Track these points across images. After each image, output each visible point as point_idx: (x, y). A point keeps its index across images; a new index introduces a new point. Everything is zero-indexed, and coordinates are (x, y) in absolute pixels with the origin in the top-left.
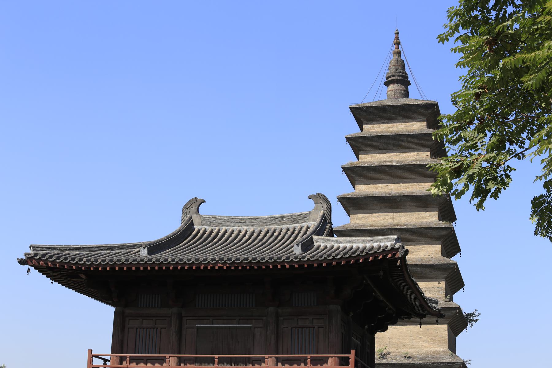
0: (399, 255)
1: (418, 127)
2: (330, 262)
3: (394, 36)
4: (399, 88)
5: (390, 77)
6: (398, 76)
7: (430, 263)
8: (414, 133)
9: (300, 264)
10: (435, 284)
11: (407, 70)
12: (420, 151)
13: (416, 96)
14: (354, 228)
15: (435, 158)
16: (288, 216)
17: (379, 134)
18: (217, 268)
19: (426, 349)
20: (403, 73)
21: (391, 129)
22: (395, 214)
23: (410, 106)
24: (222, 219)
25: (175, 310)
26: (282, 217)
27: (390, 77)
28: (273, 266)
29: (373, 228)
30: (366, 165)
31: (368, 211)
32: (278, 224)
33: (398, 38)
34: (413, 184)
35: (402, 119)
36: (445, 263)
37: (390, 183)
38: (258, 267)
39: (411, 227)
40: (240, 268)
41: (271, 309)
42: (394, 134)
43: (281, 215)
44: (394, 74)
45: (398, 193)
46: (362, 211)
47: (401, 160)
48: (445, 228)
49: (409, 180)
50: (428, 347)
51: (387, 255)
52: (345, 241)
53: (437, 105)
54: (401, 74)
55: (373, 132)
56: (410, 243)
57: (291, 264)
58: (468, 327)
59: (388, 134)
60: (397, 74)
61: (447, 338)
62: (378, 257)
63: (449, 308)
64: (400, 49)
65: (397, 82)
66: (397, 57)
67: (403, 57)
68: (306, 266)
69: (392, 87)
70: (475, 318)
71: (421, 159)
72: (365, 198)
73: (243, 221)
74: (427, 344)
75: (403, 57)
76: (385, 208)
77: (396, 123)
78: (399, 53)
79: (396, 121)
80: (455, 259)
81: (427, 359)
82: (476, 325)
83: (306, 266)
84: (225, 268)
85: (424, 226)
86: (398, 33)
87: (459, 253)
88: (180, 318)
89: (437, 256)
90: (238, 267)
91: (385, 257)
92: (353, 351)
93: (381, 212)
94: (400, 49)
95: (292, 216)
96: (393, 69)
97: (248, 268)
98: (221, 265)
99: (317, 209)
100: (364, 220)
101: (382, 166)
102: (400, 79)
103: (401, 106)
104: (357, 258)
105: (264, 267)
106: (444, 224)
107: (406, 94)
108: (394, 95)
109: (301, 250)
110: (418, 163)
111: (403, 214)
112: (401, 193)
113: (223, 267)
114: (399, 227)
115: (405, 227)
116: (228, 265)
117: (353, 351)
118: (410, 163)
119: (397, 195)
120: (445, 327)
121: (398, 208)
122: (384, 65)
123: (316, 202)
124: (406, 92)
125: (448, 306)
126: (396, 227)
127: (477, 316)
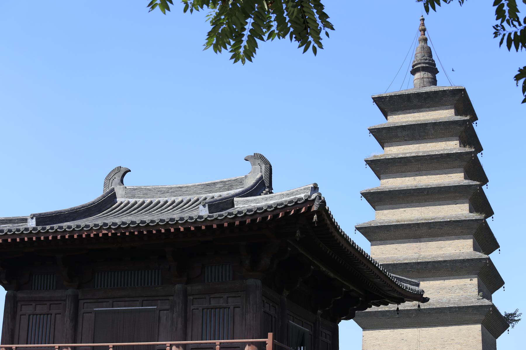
0: (315, 208)
1: (446, 114)
2: (232, 221)
3: (420, 22)
4: (426, 76)
6: (424, 63)
7: (460, 258)
8: (441, 121)
9: (196, 225)
10: (467, 281)
11: (434, 58)
12: (449, 140)
13: (445, 82)
14: (379, 224)
15: (464, 147)
16: (221, 182)
17: (404, 124)
18: (101, 235)
20: (430, 60)
21: (417, 119)
22: (423, 208)
23: (436, 93)
24: (148, 189)
25: (70, 292)
28: (165, 230)
29: (398, 223)
30: (390, 157)
31: (394, 206)
32: (210, 192)
33: (423, 25)
34: (441, 176)
35: (429, 107)
36: (477, 257)
37: (417, 175)
38: (147, 231)
39: (439, 220)
40: (127, 234)
41: (178, 287)
42: (419, 123)
43: (213, 182)
44: (419, 61)
45: (425, 185)
46: (388, 206)
47: (429, 150)
48: (476, 220)
49: (437, 171)
51: (301, 209)
52: (263, 199)
53: (464, 90)
54: (427, 61)
55: (397, 123)
56: (439, 238)
57: (186, 226)
58: (510, 328)
59: (413, 123)
60: (423, 61)
61: (480, 338)
62: (290, 212)
63: (482, 306)
64: (426, 36)
65: (424, 69)
66: (423, 44)
67: (429, 44)
68: (203, 227)
69: (418, 75)
70: (516, 318)
71: (449, 148)
72: (390, 192)
73: (170, 191)
76: (412, 202)
77: (422, 112)
78: (425, 40)
79: (422, 110)
80: (494, 257)
82: (517, 325)
83: (203, 227)
84: (110, 234)
85: (453, 219)
87: (498, 250)
88: (76, 301)
89: (468, 251)
90: (125, 233)
91: (298, 211)
92: (270, 335)
93: (408, 207)
94: (426, 36)
96: (419, 56)
97: (136, 233)
98: (106, 232)
99: (254, 172)
100: (391, 216)
102: (428, 67)
103: (426, 93)
104: (264, 215)
105: (154, 232)
106: (475, 216)
107: (434, 82)
109: (208, 212)
110: (445, 152)
111: (431, 208)
112: (429, 185)
113: (108, 234)
114: (426, 221)
115: (432, 221)
116: (113, 231)
117: (270, 335)
118: (437, 153)
119: (424, 187)
120: (479, 327)
121: (426, 201)
122: (412, 54)
123: (253, 164)
124: (433, 80)
125: (481, 304)
126: (423, 221)
127: (518, 316)
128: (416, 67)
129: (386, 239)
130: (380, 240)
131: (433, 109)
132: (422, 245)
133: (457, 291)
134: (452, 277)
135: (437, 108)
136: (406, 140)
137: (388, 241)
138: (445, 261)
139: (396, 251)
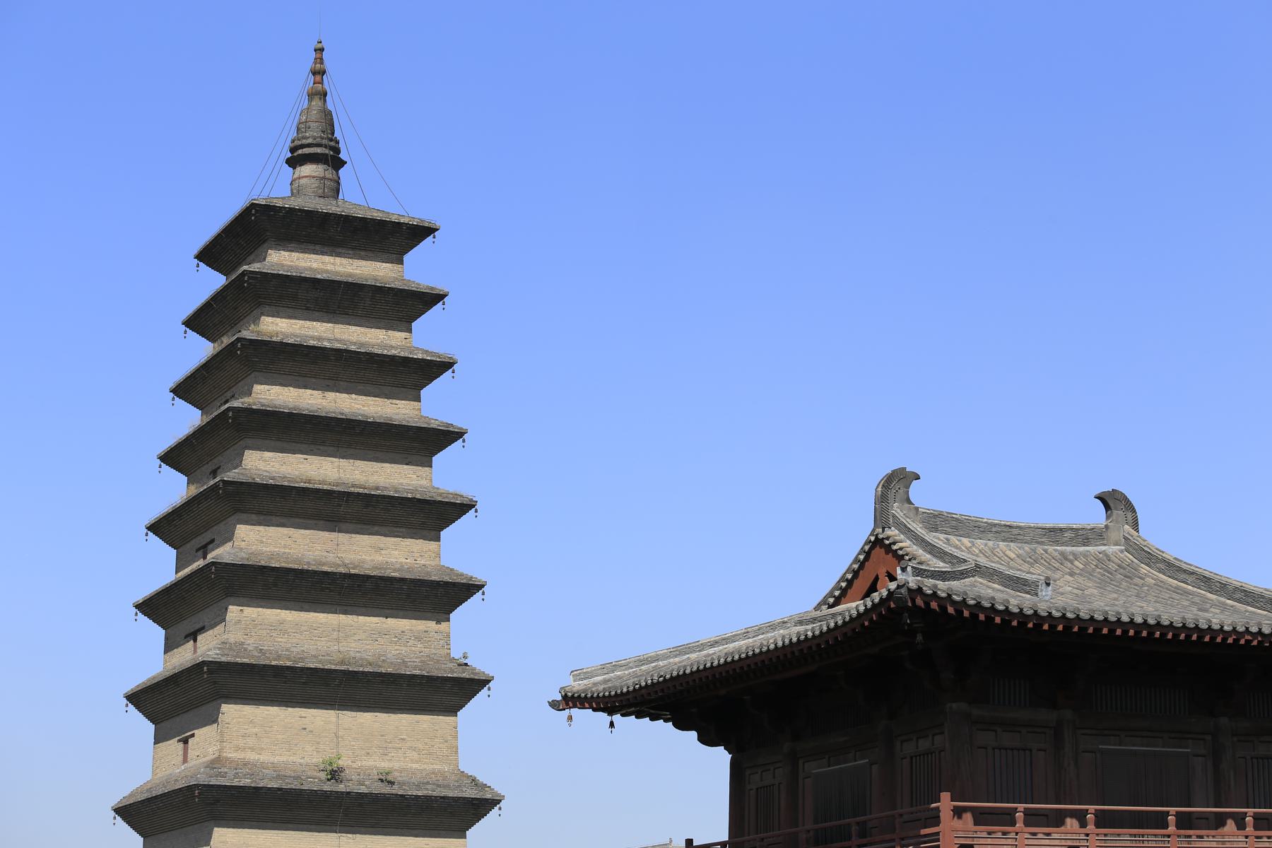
5: (302, 146)
6: (326, 147)
17: (319, 277)
19: (415, 766)
20: (331, 140)
26: (1061, 529)
27: (302, 146)
29: (311, 486)
35: (353, 248)
42: (350, 280)
50: (417, 762)
59: (338, 278)
72: (290, 415)
74: (415, 755)
75: (330, 106)
81: (429, 787)
85: (418, 496)
86: (322, 50)
95: (1077, 530)
100: (277, 466)
101: (325, 349)
108: (318, 187)
114: (366, 491)
115: (379, 492)
128: (300, 152)
129: (270, 513)
130: (259, 513)
131: (363, 253)
132: (342, 537)
133: (411, 642)
134: (401, 613)
135: (370, 254)
136: (307, 309)
137: (274, 518)
138: (402, 580)
139: (289, 542)
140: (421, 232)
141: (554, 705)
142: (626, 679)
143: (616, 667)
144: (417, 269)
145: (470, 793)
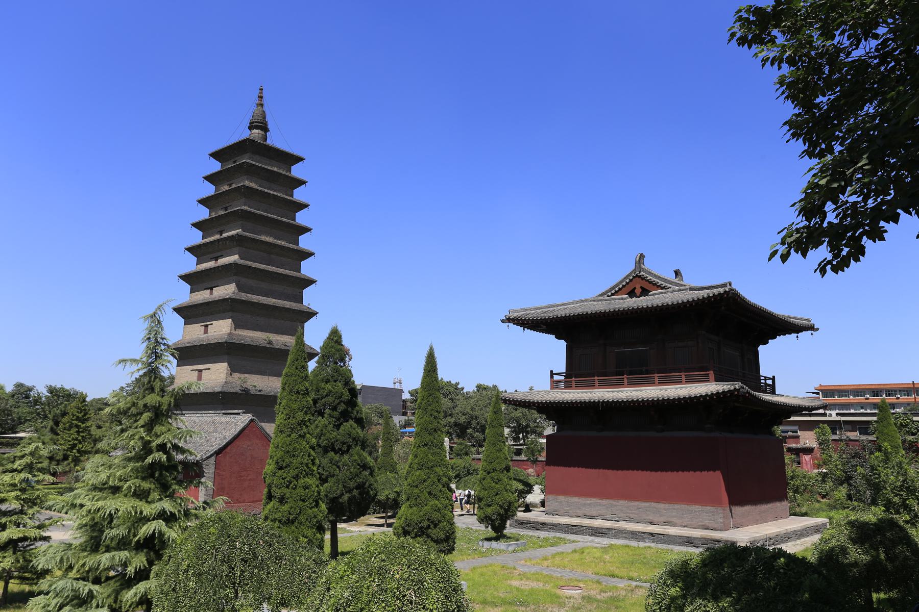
69: (255, 131)
140: (299, 159)
141: (503, 321)
142: (532, 315)
143: (527, 310)
144: (297, 171)
145: (311, 351)
